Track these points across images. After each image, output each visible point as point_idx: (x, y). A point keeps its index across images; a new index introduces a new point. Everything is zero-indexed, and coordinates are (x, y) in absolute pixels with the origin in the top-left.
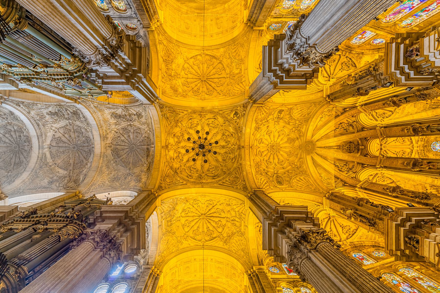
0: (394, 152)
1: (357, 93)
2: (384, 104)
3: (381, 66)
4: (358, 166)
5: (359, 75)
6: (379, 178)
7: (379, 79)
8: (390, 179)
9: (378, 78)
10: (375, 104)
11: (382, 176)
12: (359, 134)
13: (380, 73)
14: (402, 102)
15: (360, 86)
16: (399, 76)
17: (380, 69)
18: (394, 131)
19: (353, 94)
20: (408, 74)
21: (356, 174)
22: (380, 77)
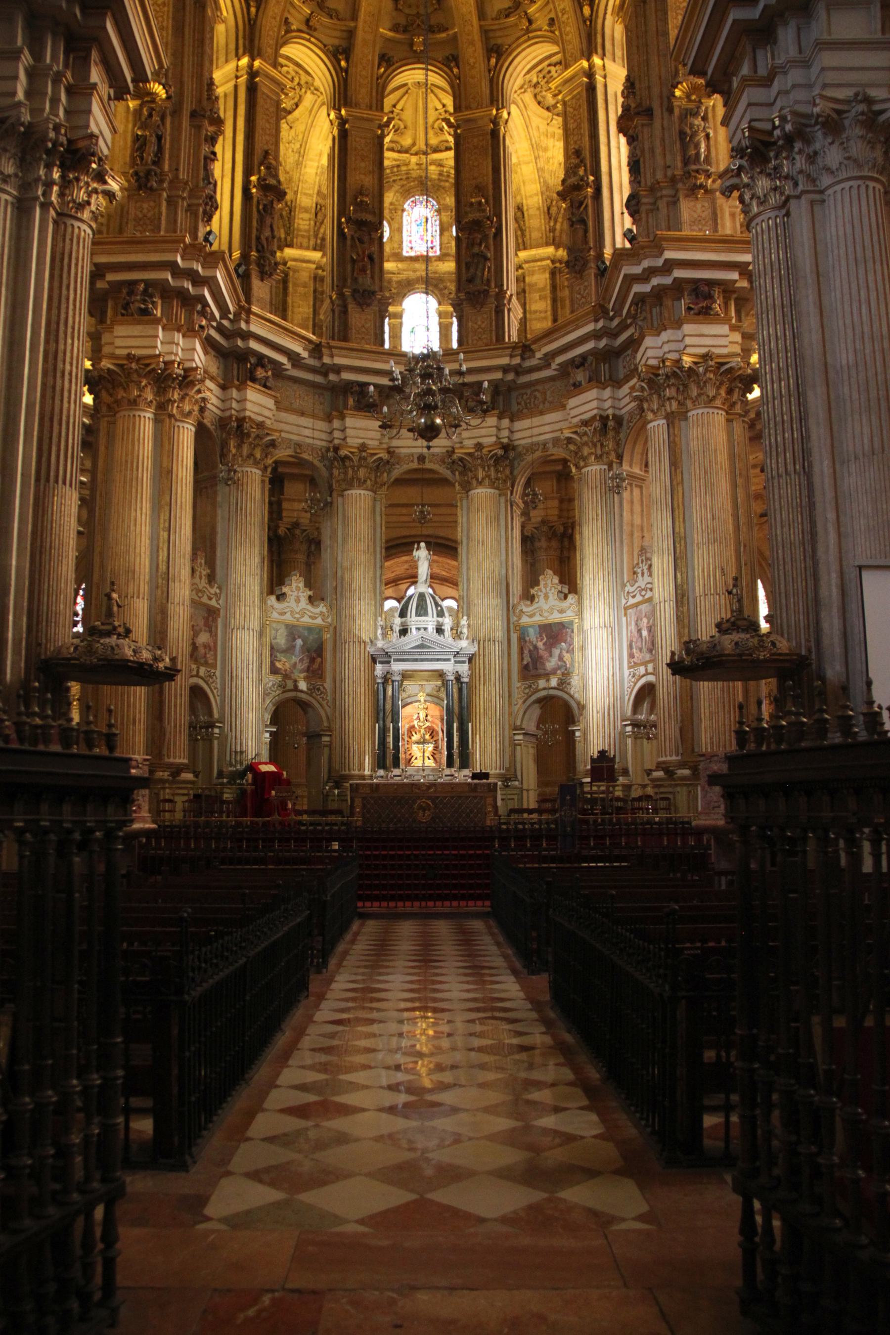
0: (399, 107)
1: (633, 105)
2: (578, 153)
3: (699, 206)
4: (338, 34)
5: (694, 134)
6: (293, 74)
7: (659, 194)
8: (297, 105)
9: (664, 192)
10: (585, 126)
11: (302, 82)
12: (476, 36)
13: (678, 199)
14: (572, 206)
15: (657, 123)
16: (646, 264)
17: (692, 204)
18: (476, 164)
19: (637, 85)
20: (646, 279)
21: (304, 28)
22: (665, 199)
